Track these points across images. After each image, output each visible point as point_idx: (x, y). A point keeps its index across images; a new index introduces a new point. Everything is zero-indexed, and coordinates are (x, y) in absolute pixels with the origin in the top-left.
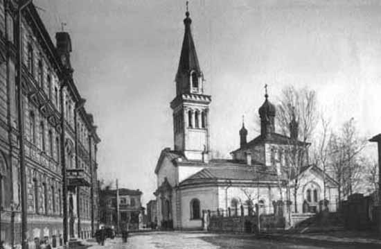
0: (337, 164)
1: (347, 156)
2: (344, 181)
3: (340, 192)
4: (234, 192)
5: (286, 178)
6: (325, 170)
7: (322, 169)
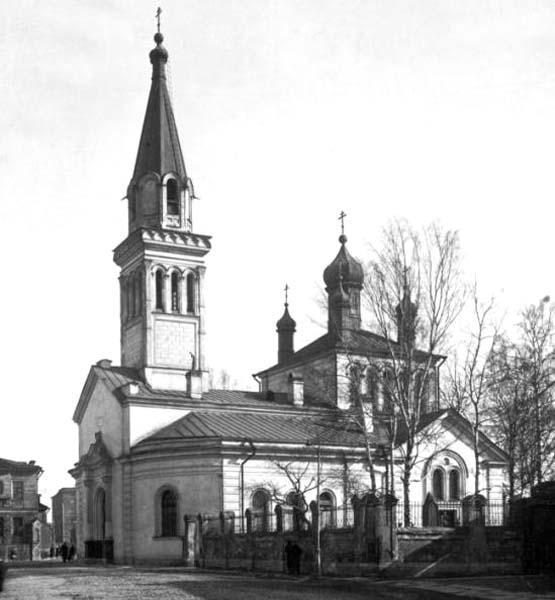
0: (508, 411)
1: (530, 392)
2: (524, 451)
3: (512, 478)
4: (260, 473)
5: (384, 441)
6: (478, 424)
7: (472, 420)
